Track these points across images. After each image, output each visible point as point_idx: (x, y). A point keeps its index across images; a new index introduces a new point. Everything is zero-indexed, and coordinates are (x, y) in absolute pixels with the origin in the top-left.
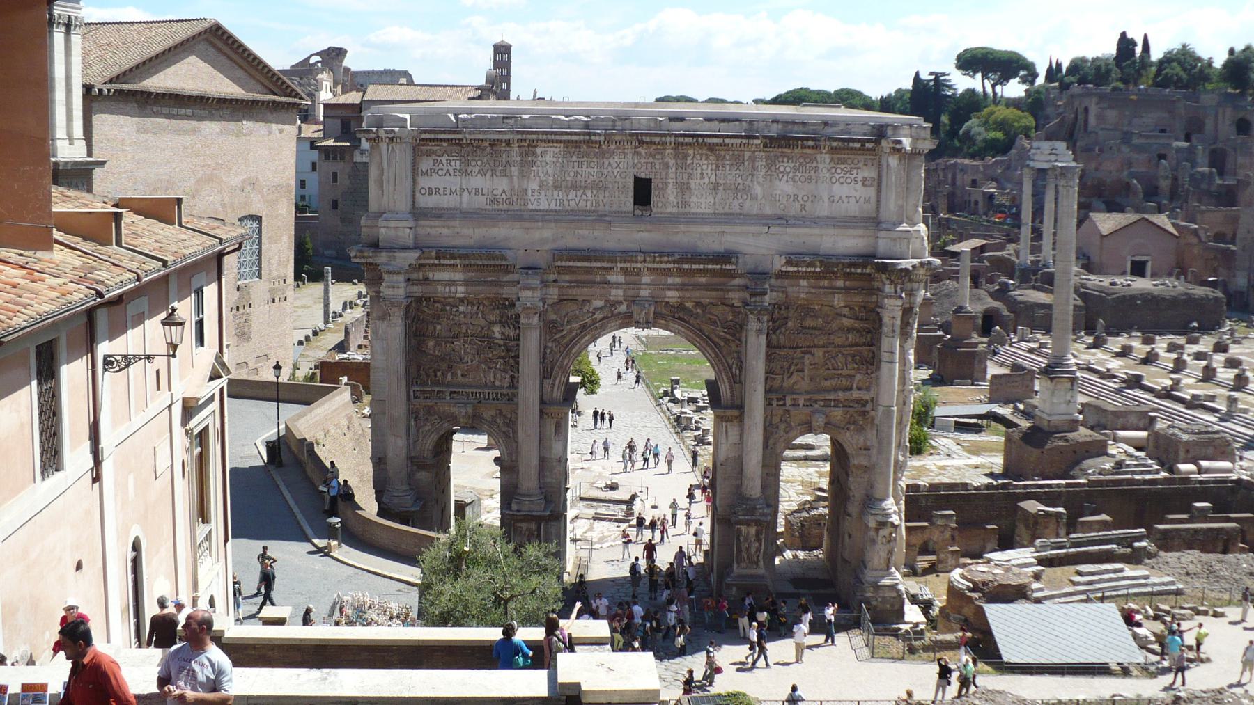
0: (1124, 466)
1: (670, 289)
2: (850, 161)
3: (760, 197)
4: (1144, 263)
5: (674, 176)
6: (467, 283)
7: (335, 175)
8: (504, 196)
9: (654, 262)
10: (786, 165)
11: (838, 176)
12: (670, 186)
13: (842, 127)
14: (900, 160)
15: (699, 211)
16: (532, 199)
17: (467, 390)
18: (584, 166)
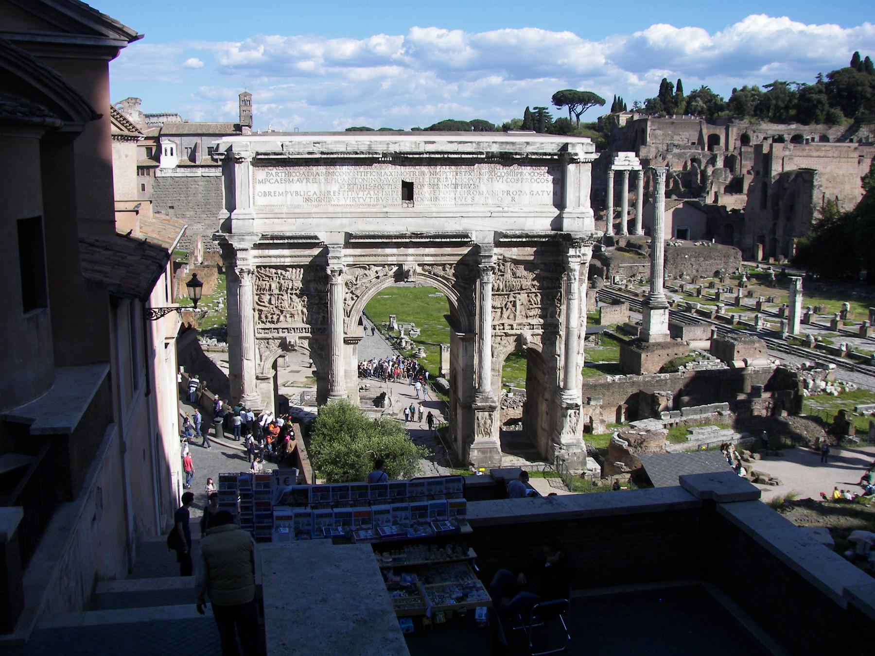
0: (700, 363)
1: (426, 255)
3: (485, 192)
4: (685, 231)
5: (427, 180)
7: (143, 185)
8: (315, 195)
9: (417, 238)
10: (501, 171)
11: (535, 178)
12: (426, 187)
13: (538, 145)
14: (576, 167)
15: (445, 203)
16: (334, 197)
17: (293, 327)
18: (369, 175)
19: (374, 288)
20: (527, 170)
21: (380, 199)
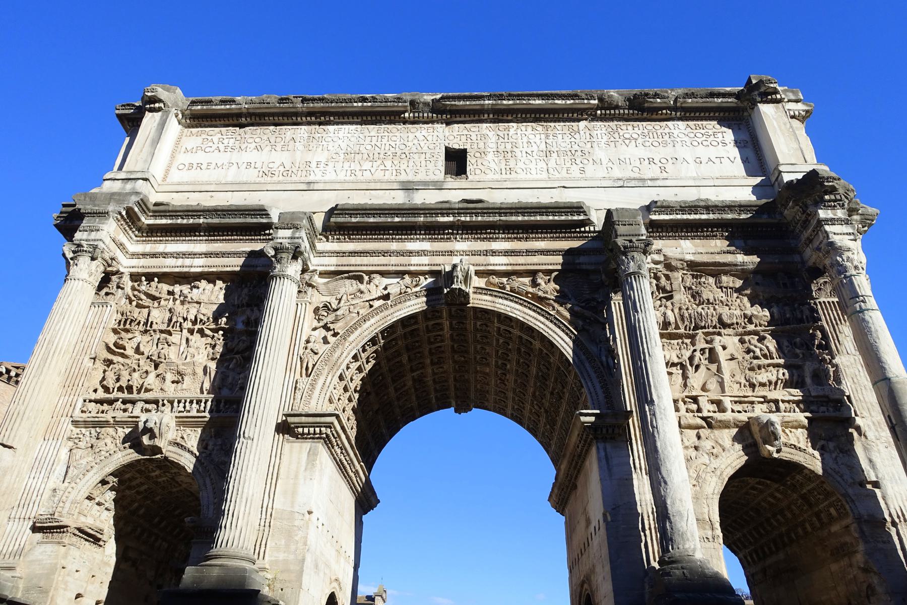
1: (494, 253)
2: (711, 127)
3: (605, 161)
5: (494, 146)
6: (208, 255)
8: (282, 168)
12: (490, 156)
14: (777, 108)
15: (529, 176)
16: (317, 170)
18: (385, 141)
19: (377, 318)
20: (679, 128)
21: (403, 172)
